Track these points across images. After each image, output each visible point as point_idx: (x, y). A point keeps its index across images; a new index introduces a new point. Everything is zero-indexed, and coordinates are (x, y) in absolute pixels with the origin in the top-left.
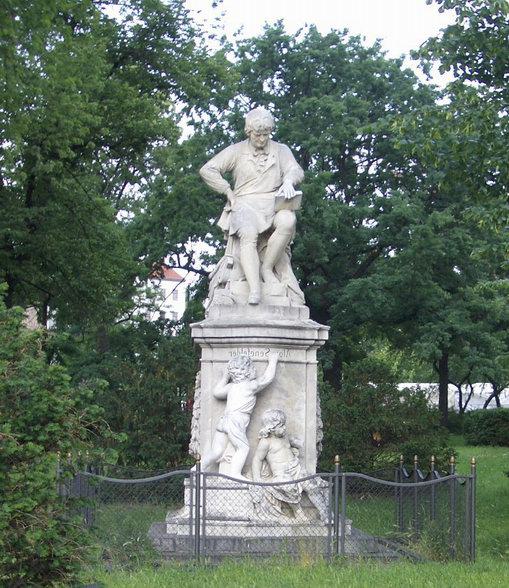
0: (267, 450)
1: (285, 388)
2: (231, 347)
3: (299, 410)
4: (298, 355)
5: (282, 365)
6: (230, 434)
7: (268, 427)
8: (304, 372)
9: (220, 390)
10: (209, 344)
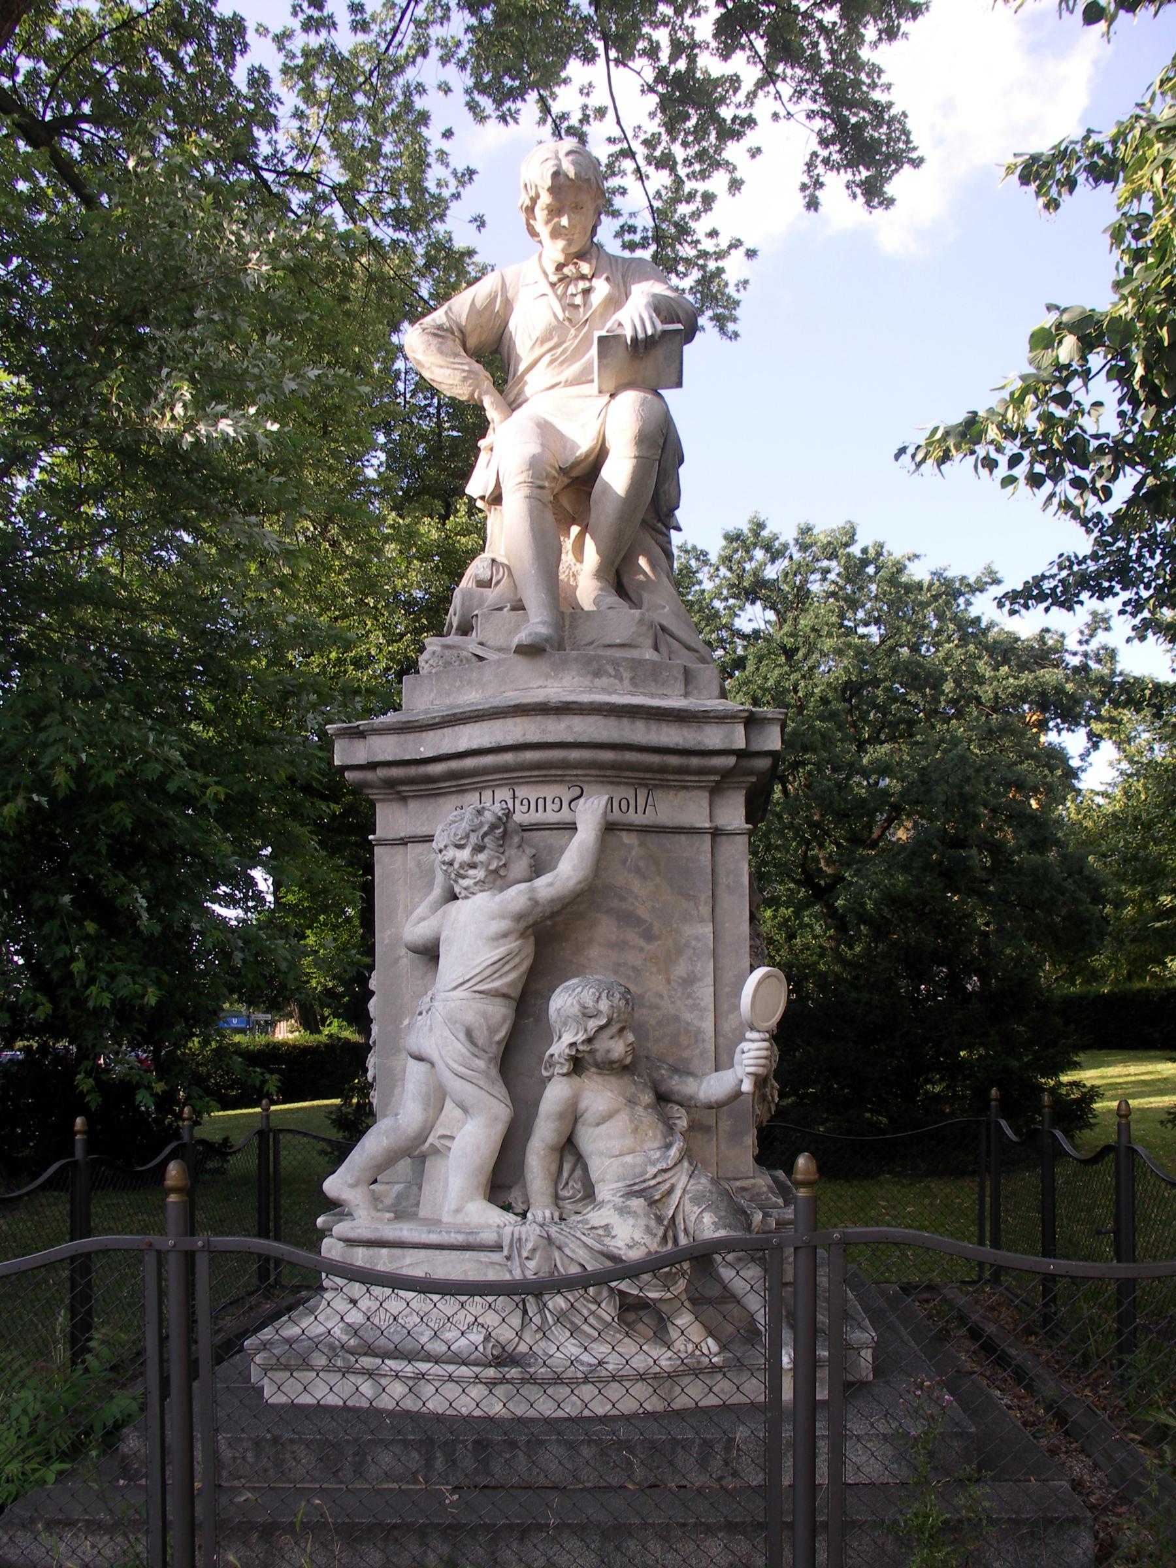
0: (572, 1117)
1: (642, 912)
2: (461, 791)
3: (689, 981)
4: (693, 810)
5: (628, 839)
6: (440, 1064)
7: (568, 1038)
8: (706, 859)
10: (390, 784)
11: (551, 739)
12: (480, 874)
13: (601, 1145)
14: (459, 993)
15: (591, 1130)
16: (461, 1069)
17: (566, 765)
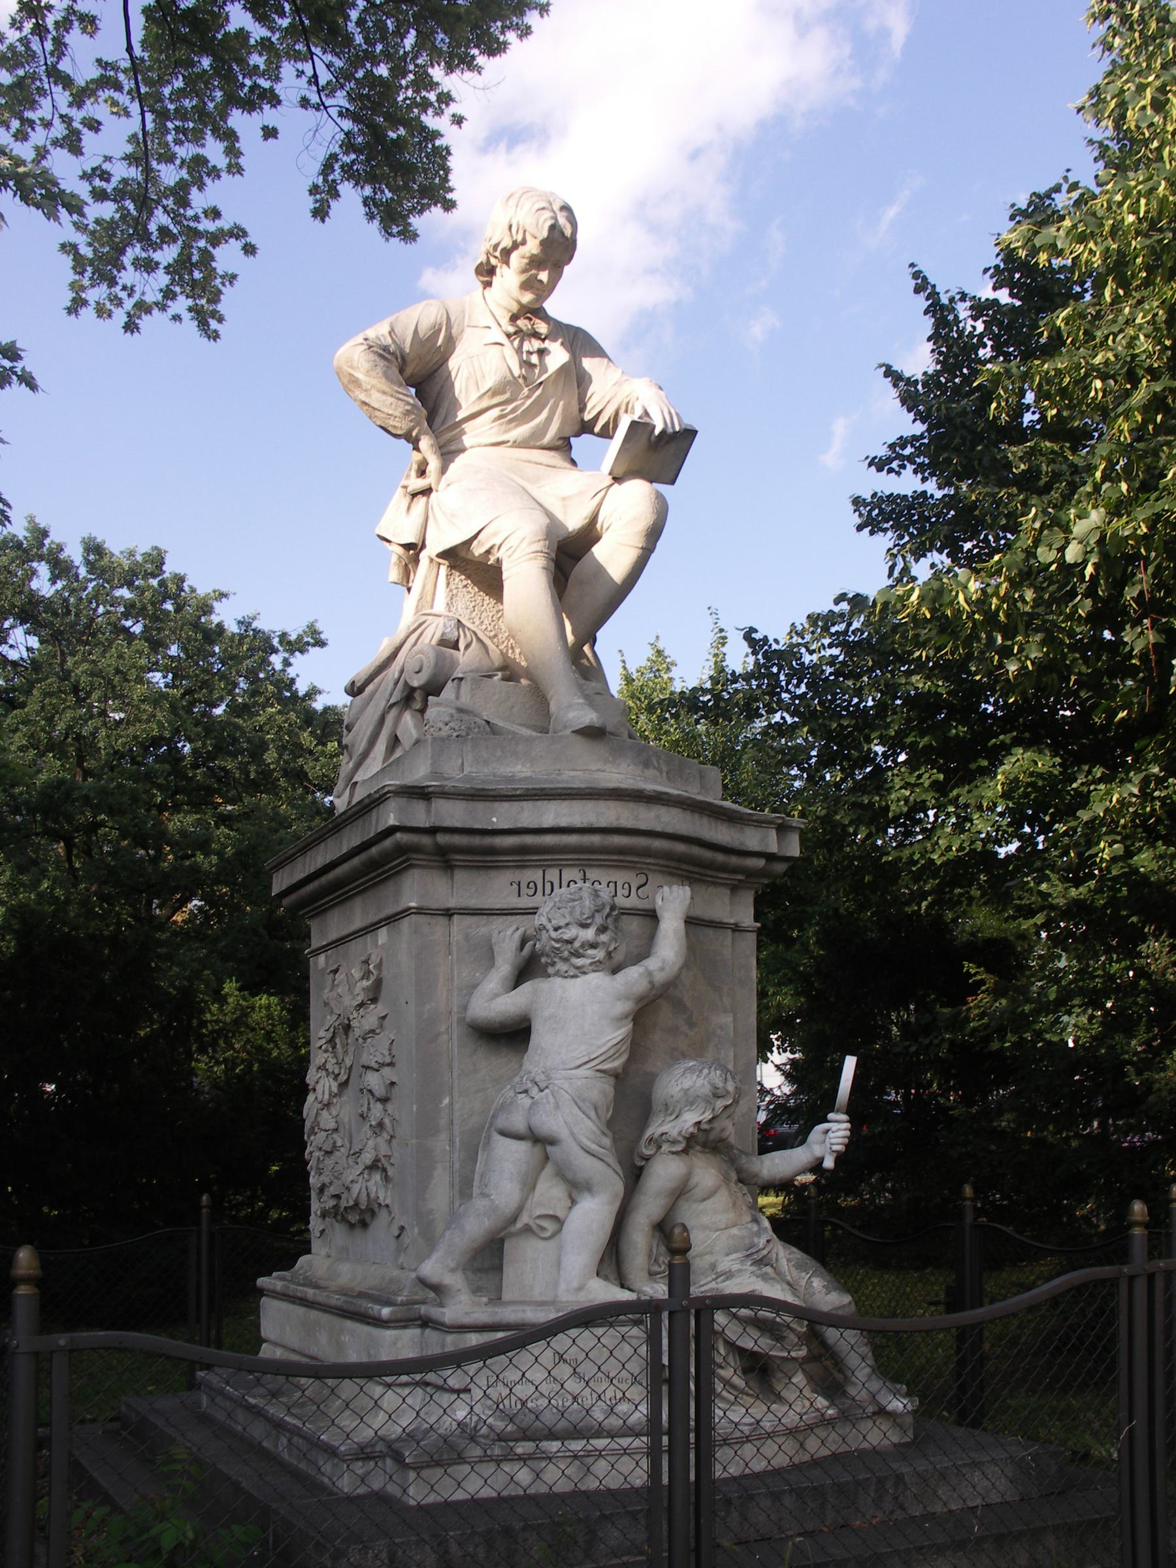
0: (681, 1192)
2: (522, 866)
9: (495, 1001)
11: (643, 826)
12: (599, 954)
13: (705, 1220)
14: (582, 1072)
15: (695, 1206)
16: (594, 1147)
17: (646, 852)
